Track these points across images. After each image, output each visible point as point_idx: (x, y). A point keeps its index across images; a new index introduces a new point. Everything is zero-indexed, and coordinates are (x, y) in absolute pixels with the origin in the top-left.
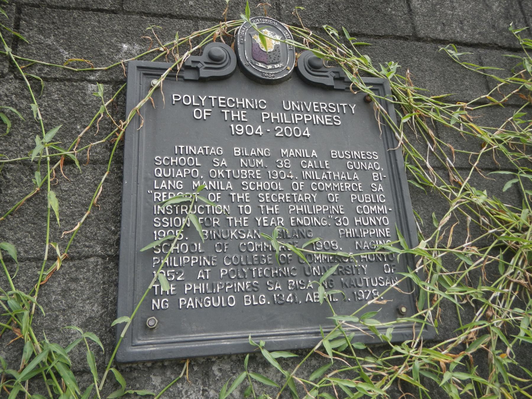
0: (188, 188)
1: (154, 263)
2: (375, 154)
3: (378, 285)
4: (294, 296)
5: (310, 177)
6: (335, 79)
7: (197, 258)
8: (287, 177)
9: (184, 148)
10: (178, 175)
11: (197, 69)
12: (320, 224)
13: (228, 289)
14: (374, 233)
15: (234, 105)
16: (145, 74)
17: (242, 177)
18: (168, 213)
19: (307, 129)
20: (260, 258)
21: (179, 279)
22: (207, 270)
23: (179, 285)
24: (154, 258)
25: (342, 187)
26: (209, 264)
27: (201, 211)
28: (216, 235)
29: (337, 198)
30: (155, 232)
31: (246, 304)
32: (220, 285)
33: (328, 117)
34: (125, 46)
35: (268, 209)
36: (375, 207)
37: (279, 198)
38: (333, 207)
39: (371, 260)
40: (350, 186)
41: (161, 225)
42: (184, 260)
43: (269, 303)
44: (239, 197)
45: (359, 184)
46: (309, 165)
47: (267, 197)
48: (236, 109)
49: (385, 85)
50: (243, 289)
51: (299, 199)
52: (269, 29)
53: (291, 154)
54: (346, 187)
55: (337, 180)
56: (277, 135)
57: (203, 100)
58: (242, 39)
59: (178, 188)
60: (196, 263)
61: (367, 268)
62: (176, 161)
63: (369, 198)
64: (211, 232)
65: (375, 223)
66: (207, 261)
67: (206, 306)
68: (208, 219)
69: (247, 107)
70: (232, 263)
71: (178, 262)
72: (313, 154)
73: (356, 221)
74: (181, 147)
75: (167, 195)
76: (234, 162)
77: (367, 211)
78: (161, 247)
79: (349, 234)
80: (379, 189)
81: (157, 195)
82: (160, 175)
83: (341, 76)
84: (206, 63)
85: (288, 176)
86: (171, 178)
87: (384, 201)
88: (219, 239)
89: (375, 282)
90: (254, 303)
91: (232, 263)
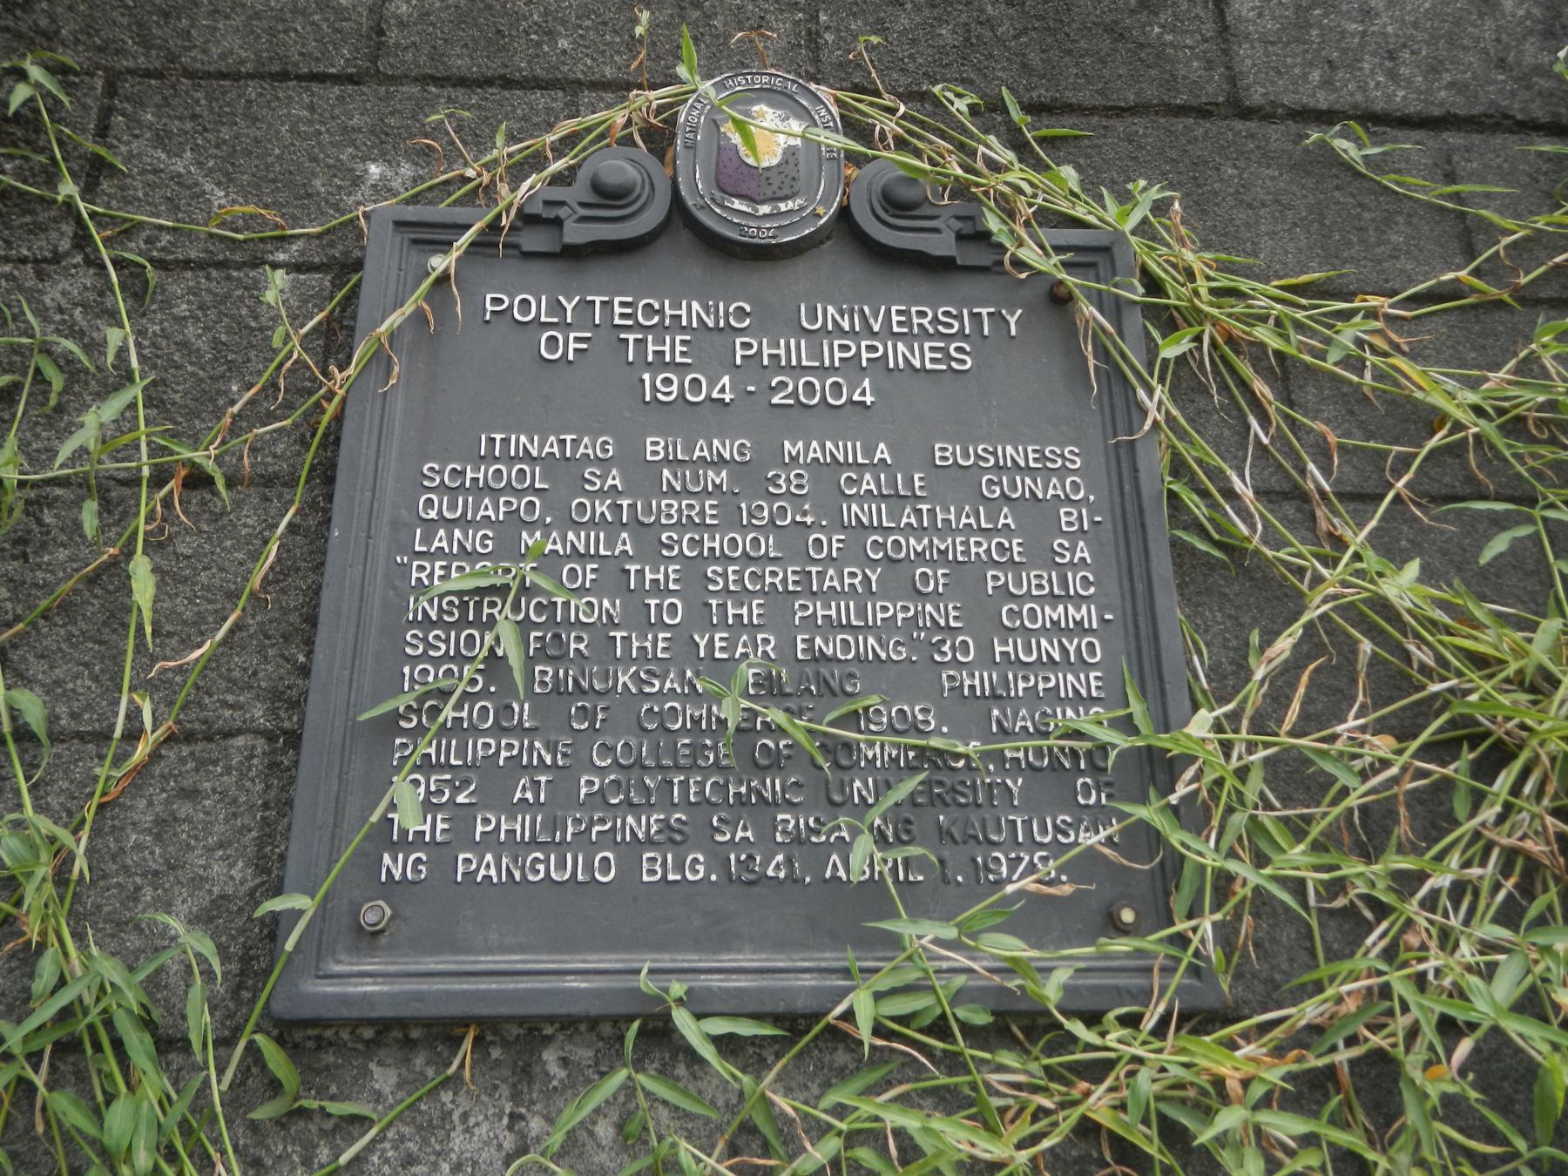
0: (507, 548)
1: (397, 755)
2: (1071, 452)
3: (1055, 837)
4: (789, 861)
5: (865, 520)
6: (960, 237)
7: (516, 743)
8: (794, 521)
9: (506, 441)
10: (482, 513)
11: (557, 223)
12: (883, 656)
13: (599, 833)
14: (1052, 684)
15: (656, 319)
16: (415, 242)
17: (664, 521)
18: (446, 618)
19: (866, 383)
20: (697, 750)
21: (461, 799)
22: (543, 779)
23: (462, 818)
24: (398, 741)
25: (960, 548)
26: (548, 761)
27: (538, 614)
28: (575, 681)
29: (941, 581)
30: (406, 670)
31: (645, 878)
32: (577, 821)
33: (932, 349)
34: (374, 170)
35: (731, 612)
36: (1061, 608)
37: (768, 580)
38: (929, 608)
39: (1037, 764)
40: (985, 546)
41: (425, 652)
42: (479, 747)
43: (713, 877)
44: (649, 576)
45: (1015, 542)
46: (865, 487)
47: (731, 578)
48: (660, 330)
49: (1116, 250)
50: (640, 836)
51: (827, 584)
52: (771, 104)
53: (811, 455)
54: (973, 550)
55: (948, 529)
56: (775, 400)
57: (569, 308)
58: (691, 136)
59: (480, 550)
60: (512, 757)
61: (1021, 788)
62: (481, 476)
63: (1044, 582)
64: (561, 672)
65: (1057, 657)
66: (543, 753)
67: (531, 878)
68: (557, 636)
69: (695, 325)
70: (616, 761)
71: (462, 752)
72: (878, 455)
73: (998, 649)
74: (498, 437)
75: (447, 568)
76: (643, 478)
77: (1034, 618)
78: (418, 712)
79: (972, 687)
80: (1078, 555)
81: (421, 568)
82: (433, 514)
83: (979, 228)
84: (583, 205)
85: (798, 519)
86: (463, 522)
87: (1092, 590)
88: (584, 692)
89: (1044, 831)
90: (671, 877)
91: (616, 761)
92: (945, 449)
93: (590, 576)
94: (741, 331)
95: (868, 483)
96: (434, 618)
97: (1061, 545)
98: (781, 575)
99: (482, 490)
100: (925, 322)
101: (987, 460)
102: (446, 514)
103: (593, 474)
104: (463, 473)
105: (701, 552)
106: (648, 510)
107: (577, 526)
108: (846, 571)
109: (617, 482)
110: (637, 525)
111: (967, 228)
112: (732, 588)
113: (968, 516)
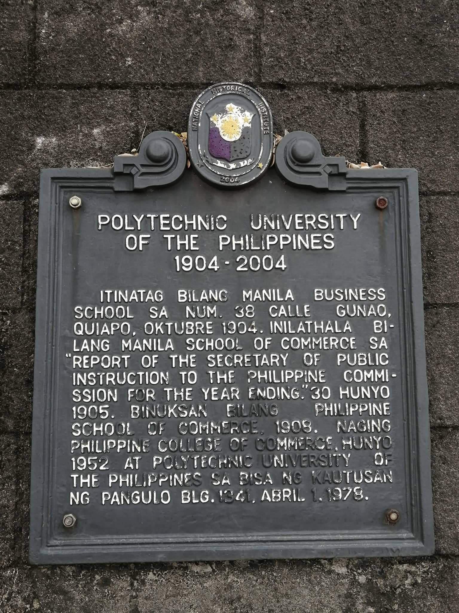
0: (116, 349)
1: (73, 448)
2: (381, 291)
3: (364, 481)
4: (246, 493)
5: (281, 330)
6: (331, 175)
7: (125, 442)
8: (247, 331)
9: (112, 294)
10: (103, 331)
11: (131, 175)
12: (288, 397)
13: (162, 482)
14: (366, 409)
15: (181, 226)
16: (62, 187)
17: (187, 333)
18: (90, 383)
19: (282, 258)
20: (205, 443)
21: (102, 468)
22: (137, 458)
23: (103, 477)
24: (73, 442)
25: (325, 343)
26: (139, 450)
27: (132, 381)
28: (150, 412)
29: (316, 360)
30: (74, 409)
31: (183, 502)
32: (153, 477)
33: (315, 238)
34: (40, 141)
35: (219, 377)
36: (372, 372)
37: (236, 361)
38: (310, 373)
39: (357, 447)
40: (337, 341)
41: (82, 400)
42: (108, 444)
43: (213, 501)
44: (181, 360)
45: (351, 339)
46: (281, 313)
47: (219, 360)
48: (183, 233)
49: (408, 180)
50: (181, 483)
51: (263, 362)
52: (236, 104)
53: (256, 297)
54: (332, 343)
55: (320, 334)
56: (239, 269)
57: (139, 221)
58: (195, 124)
59: (103, 349)
60: (123, 448)
61: (349, 458)
62: (102, 312)
63: (365, 359)
64: (143, 408)
65: (369, 396)
66: (136, 446)
67: (134, 502)
68: (140, 391)
69: (200, 229)
70: (169, 449)
71: (101, 447)
72: (287, 296)
73: (341, 392)
74: (109, 292)
75: (89, 359)
76: (177, 311)
77: (358, 377)
78: (81, 428)
79: (329, 411)
80: (382, 344)
81: (77, 360)
82: (81, 333)
83: (341, 171)
84: (142, 166)
85: (250, 330)
86: (95, 337)
87: (387, 362)
88: (154, 417)
89: (359, 478)
90: (194, 501)
91: (169, 449)
92: (320, 292)
93: (154, 361)
94: (223, 232)
95: (282, 311)
96: (85, 384)
97: (373, 340)
98: (242, 358)
99: (102, 320)
100: (312, 223)
101: (339, 297)
102: (87, 332)
103: (154, 309)
104: (94, 310)
105: (205, 348)
106: (180, 328)
107: (148, 337)
108: (272, 355)
109: (165, 313)
110: (174, 336)
111: (334, 171)
112: (219, 365)
113: (329, 326)
